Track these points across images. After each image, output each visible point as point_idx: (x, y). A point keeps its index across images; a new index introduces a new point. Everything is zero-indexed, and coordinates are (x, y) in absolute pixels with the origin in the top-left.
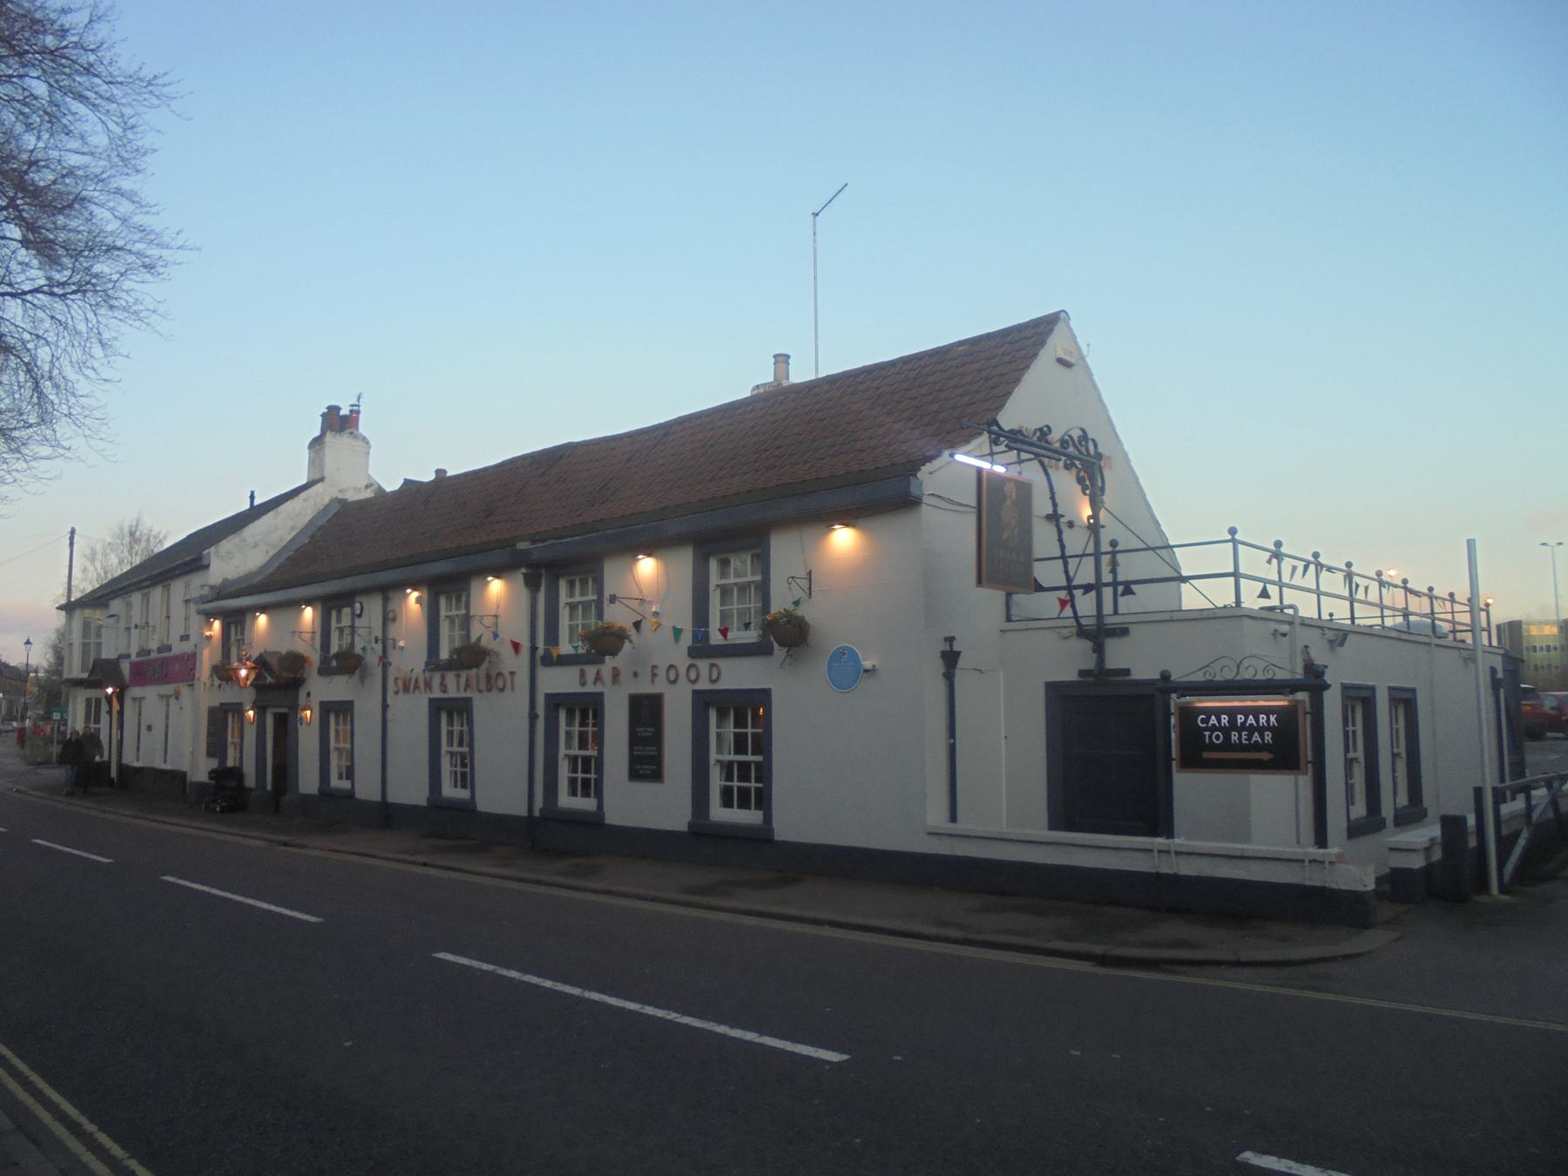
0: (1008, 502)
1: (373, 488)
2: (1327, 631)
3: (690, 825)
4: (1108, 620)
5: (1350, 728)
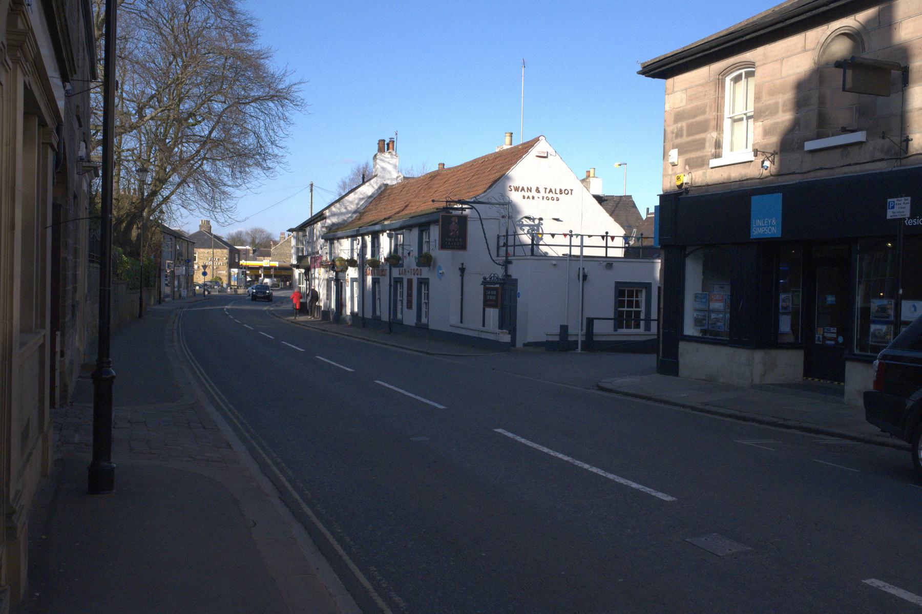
0: (453, 223)
1: (400, 178)
2: (602, 262)
3: (416, 324)
4: (509, 258)
5: (426, 292)
